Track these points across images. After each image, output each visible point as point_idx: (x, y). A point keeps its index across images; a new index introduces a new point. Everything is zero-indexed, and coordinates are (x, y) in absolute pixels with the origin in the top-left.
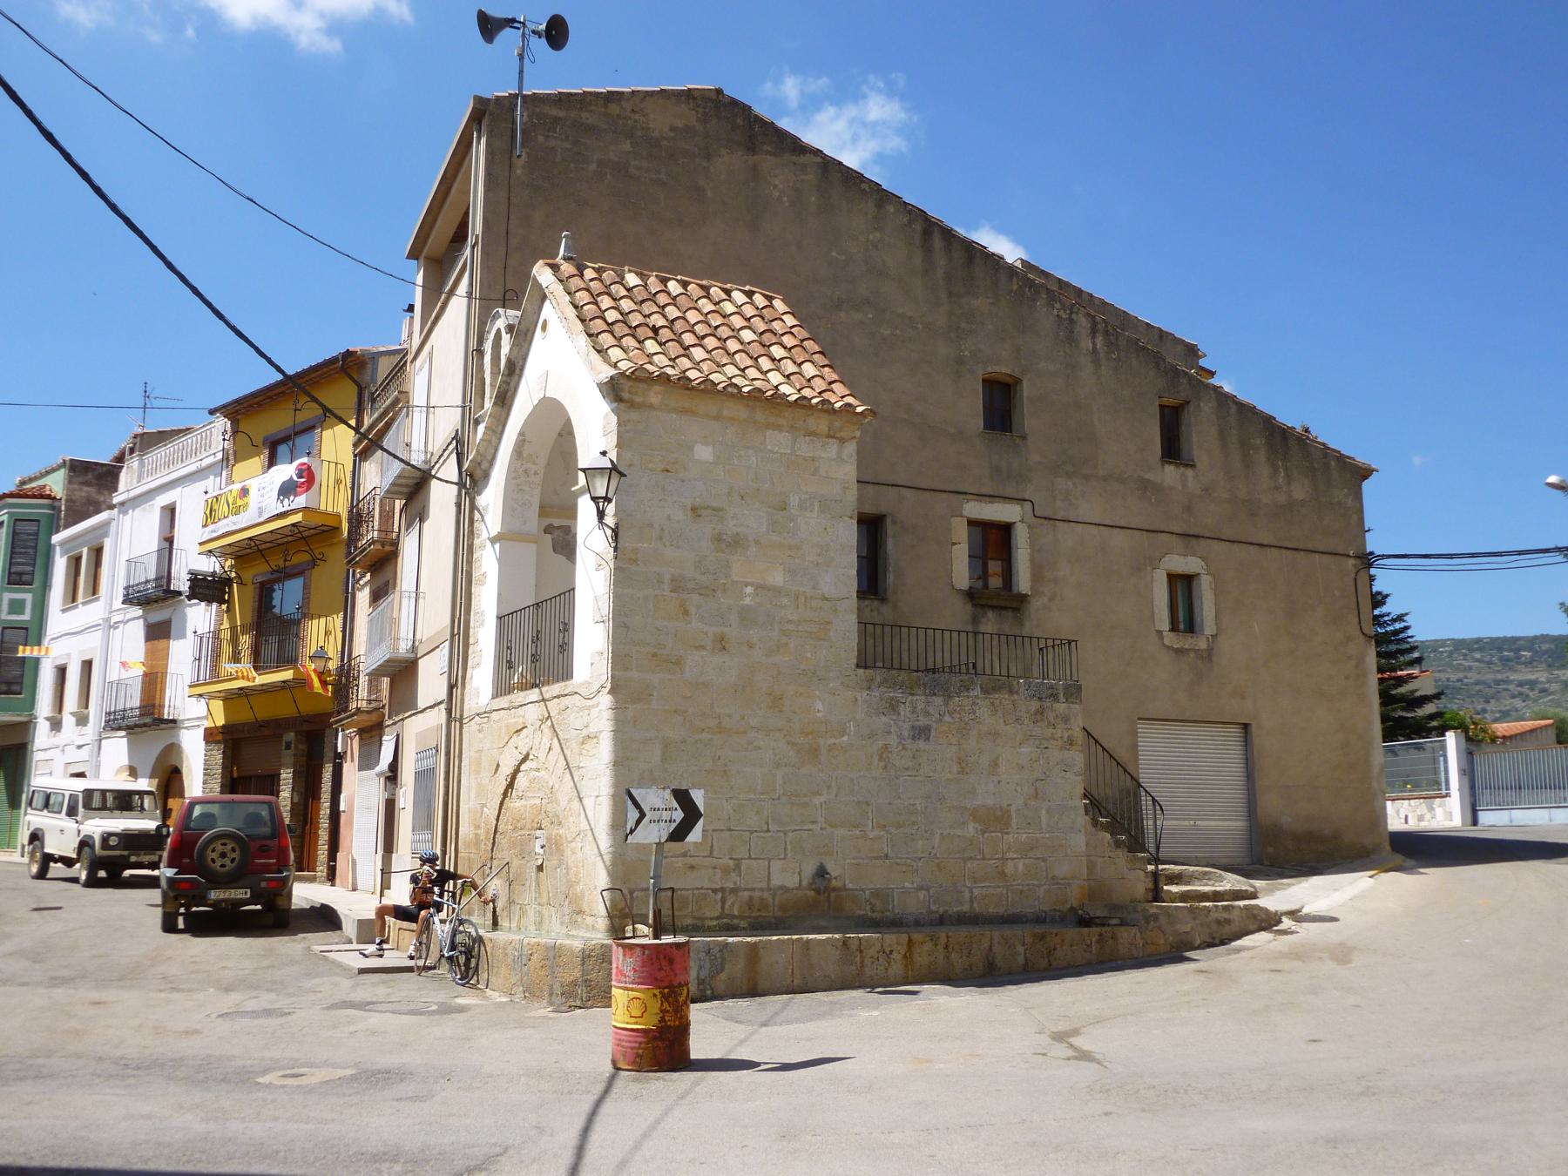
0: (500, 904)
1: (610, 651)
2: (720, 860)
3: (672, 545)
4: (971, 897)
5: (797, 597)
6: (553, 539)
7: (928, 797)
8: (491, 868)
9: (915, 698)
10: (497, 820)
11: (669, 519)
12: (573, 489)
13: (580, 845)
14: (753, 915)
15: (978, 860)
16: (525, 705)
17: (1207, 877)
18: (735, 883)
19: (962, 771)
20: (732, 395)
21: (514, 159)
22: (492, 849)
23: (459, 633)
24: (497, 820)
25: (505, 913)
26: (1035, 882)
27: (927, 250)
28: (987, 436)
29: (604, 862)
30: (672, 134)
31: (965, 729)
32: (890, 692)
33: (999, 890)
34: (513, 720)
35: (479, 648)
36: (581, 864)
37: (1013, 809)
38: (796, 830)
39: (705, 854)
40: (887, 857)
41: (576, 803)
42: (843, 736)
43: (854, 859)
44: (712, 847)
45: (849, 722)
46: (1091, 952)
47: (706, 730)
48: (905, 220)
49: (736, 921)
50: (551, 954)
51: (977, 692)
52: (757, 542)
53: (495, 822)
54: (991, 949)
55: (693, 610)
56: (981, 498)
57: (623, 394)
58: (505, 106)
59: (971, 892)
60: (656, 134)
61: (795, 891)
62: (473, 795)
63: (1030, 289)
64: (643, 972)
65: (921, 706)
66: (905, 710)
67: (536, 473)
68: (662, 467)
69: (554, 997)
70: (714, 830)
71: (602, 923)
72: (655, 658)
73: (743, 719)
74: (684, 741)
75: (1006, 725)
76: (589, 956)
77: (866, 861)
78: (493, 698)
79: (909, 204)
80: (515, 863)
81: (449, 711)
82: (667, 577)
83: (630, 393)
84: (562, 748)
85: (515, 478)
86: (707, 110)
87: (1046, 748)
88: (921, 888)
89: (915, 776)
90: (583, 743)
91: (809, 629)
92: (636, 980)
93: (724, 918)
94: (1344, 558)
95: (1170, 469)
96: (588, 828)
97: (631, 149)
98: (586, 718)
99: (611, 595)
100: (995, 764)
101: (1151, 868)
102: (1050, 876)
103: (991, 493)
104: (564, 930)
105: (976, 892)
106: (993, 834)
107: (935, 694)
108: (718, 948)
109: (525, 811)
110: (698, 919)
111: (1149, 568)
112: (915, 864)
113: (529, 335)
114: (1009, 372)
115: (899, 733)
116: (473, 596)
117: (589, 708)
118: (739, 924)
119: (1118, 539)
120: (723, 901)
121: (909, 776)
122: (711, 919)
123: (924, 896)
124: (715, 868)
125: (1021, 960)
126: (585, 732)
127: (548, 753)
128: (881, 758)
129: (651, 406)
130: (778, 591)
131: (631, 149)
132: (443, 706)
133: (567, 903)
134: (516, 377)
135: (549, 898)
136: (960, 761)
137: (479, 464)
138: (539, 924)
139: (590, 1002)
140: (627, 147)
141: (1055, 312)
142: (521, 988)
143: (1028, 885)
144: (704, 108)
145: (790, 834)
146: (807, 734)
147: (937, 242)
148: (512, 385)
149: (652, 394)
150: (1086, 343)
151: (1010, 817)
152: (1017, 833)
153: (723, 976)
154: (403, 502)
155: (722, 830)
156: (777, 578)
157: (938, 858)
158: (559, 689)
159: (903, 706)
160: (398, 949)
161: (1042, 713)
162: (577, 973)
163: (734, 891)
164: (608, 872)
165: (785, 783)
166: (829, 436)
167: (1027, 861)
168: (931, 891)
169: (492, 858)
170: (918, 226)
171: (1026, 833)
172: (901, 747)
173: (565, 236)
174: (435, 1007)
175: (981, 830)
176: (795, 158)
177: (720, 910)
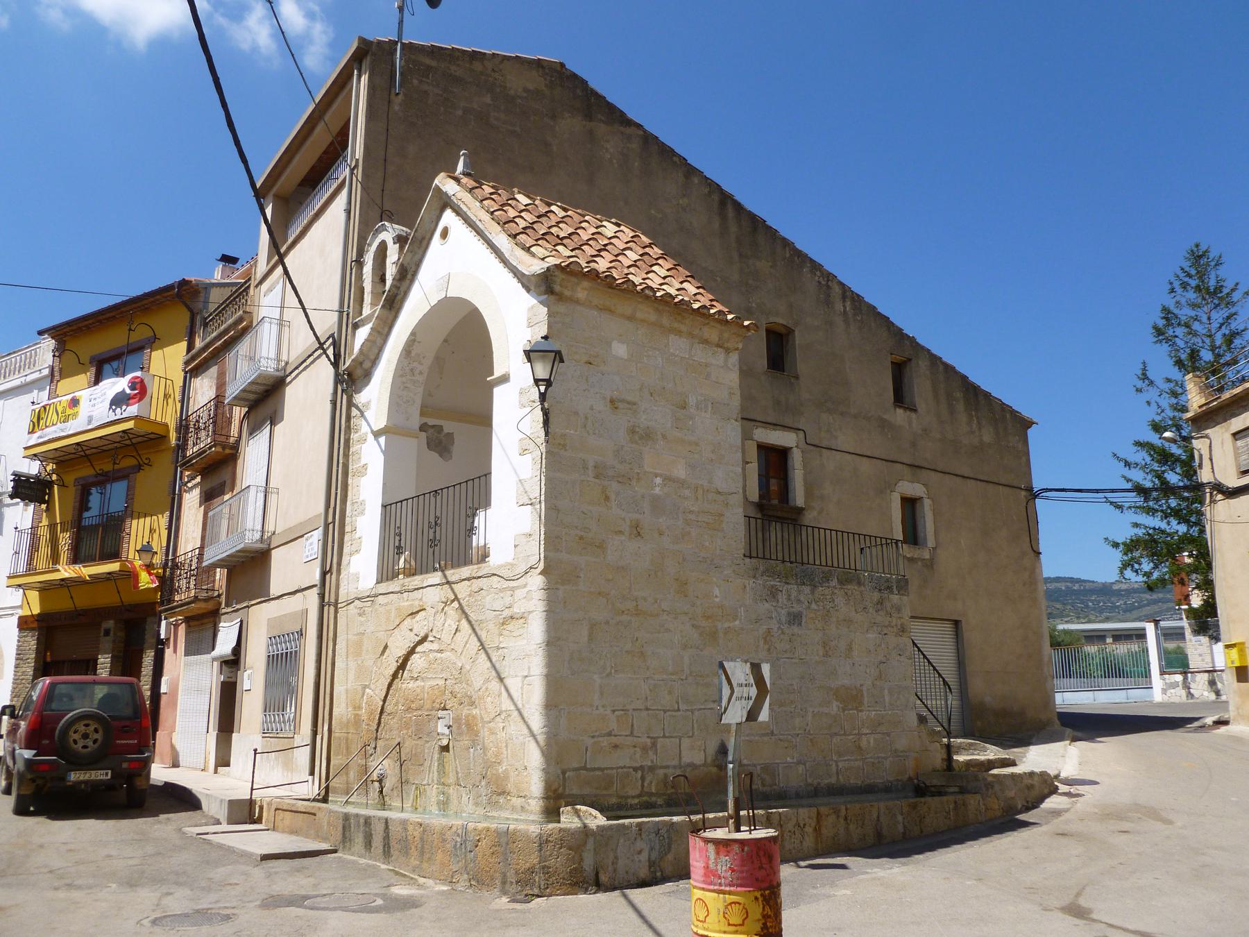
0: (388, 784)
1: (542, 533)
2: (640, 739)
3: (594, 434)
4: (837, 769)
5: (696, 488)
6: (427, 437)
7: (802, 678)
8: (375, 748)
9: (789, 587)
10: (384, 701)
11: (592, 409)
12: (488, 379)
13: (501, 725)
14: (669, 792)
15: (840, 735)
16: (422, 588)
17: (973, 748)
18: (652, 761)
19: (826, 655)
20: (647, 297)
21: (393, 96)
23: (334, 522)
24: (384, 701)
25: (395, 793)
26: (883, 755)
27: (723, 217)
28: (769, 374)
29: (537, 742)
30: (525, 95)
31: (827, 615)
32: (771, 581)
33: (857, 763)
34: (406, 604)
35: (357, 536)
36: (504, 744)
37: (864, 689)
38: (701, 709)
39: (627, 734)
40: (772, 733)
41: (495, 685)
42: (735, 620)
43: (747, 736)
44: (632, 725)
45: (740, 608)
46: (950, 818)
47: (626, 612)
48: (706, 191)
49: (654, 799)
50: (504, 840)
51: (834, 583)
52: (664, 437)
53: (381, 703)
54: (878, 820)
55: (613, 497)
56: (768, 425)
57: (555, 286)
58: (387, 49)
59: (837, 766)
60: (512, 92)
61: (702, 768)
62: (351, 676)
63: (798, 258)
64: (742, 872)
65: (794, 594)
66: (782, 598)
67: (421, 373)
68: (585, 358)
70: (634, 709)
71: (536, 805)
72: (582, 541)
73: (656, 602)
74: (607, 623)
75: (857, 613)
76: (547, 842)
77: (757, 738)
78: (377, 583)
79: (708, 178)
80: (408, 745)
81: (322, 596)
82: (591, 464)
83: (561, 286)
84: (474, 630)
85: (401, 376)
86: (553, 79)
87: (886, 634)
88: (799, 763)
89: (792, 658)
90: (503, 624)
91: (706, 520)
92: (735, 882)
93: (644, 796)
94: (1019, 490)
95: (900, 411)
96: (513, 708)
97: (491, 103)
98: (508, 600)
99: (543, 478)
100: (850, 648)
101: (945, 740)
102: (893, 748)
103: (774, 422)
104: (480, 811)
105: (841, 765)
106: (851, 712)
107: (804, 584)
108: (665, 829)
109: (423, 692)
110: (622, 797)
111: (888, 491)
112: (794, 740)
113: (425, 242)
114: (785, 323)
115: (778, 618)
116: (350, 488)
117: (513, 589)
118: (656, 801)
119: (866, 466)
120: (643, 779)
121: (788, 658)
122: (633, 797)
123: (802, 770)
124: (635, 747)
125: (901, 829)
126: (507, 613)
127: (455, 634)
128: (766, 642)
129: (577, 302)
130: (681, 483)
131: (491, 103)
132: (315, 591)
133: (483, 783)
134: (408, 282)
135: (458, 779)
136: (825, 645)
137: (361, 364)
138: (444, 805)
139: (548, 890)
140: (488, 99)
141: (817, 278)
142: (466, 876)
143: (878, 758)
144: (551, 77)
145: (696, 713)
146: (709, 617)
147: (731, 212)
148: (402, 289)
149: (579, 289)
150: (839, 306)
151: (862, 695)
152: (869, 711)
153: (670, 857)
154: (245, 410)
155: (640, 710)
156: (680, 472)
157: (810, 735)
158: (469, 572)
159: (780, 593)
160: (274, 830)
161: (882, 603)
162: (534, 859)
163: (652, 769)
164: (542, 752)
165: (691, 664)
166: (718, 346)
167: (877, 736)
168: (807, 765)
169: (376, 738)
170: (716, 197)
171: (874, 711)
172: (780, 632)
173: (463, 154)
174: (379, 902)
175: (842, 708)
176: (622, 129)
177: (640, 788)
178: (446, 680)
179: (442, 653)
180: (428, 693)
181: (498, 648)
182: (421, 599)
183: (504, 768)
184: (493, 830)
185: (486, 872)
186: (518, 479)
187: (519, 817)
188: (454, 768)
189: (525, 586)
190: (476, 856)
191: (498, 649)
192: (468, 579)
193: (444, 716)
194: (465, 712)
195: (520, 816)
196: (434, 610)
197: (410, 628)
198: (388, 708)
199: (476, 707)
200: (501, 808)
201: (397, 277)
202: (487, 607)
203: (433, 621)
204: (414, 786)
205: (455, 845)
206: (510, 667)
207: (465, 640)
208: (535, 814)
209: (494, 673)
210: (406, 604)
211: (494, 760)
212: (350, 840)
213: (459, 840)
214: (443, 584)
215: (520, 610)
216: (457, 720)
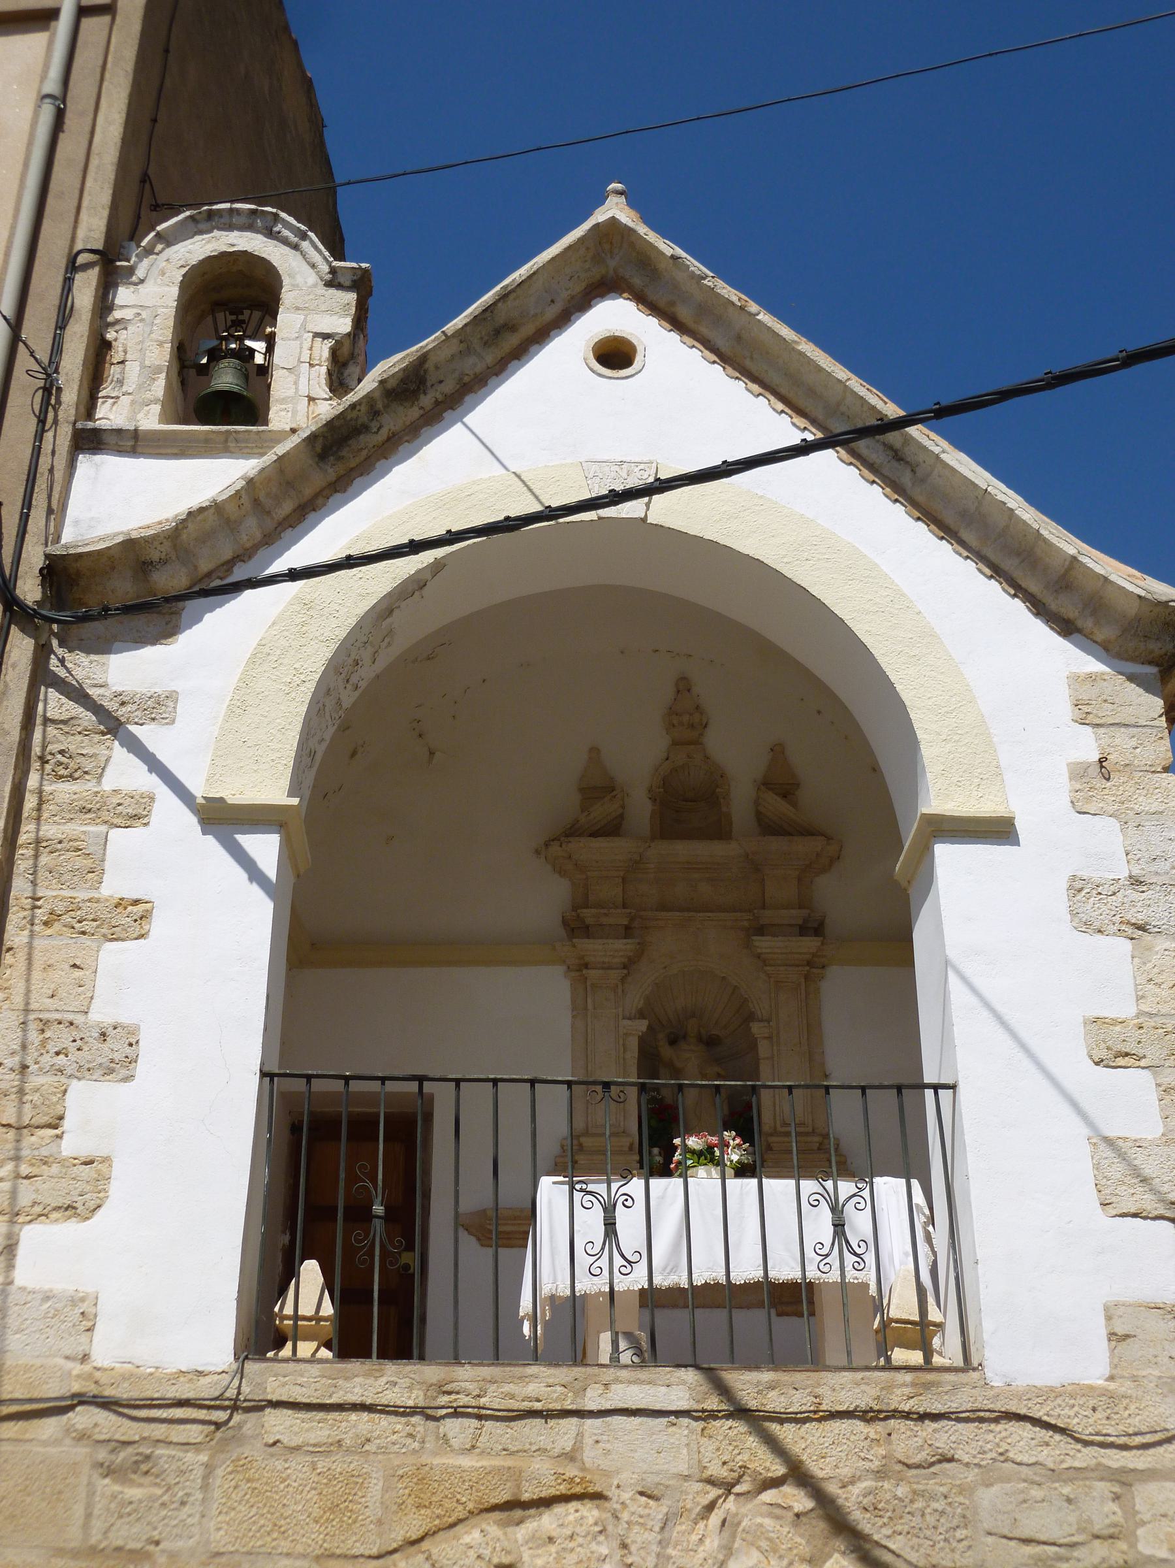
35: (72, 1145)
113: (513, 340)
117: (1124, 1479)
134: (414, 413)
158: (874, 1392)
182: (571, 1456)
192: (867, 1416)
196: (658, 1511)
201: (391, 384)
202: (986, 1526)
203: (655, 1548)
210: (466, 1462)
214: (712, 1415)
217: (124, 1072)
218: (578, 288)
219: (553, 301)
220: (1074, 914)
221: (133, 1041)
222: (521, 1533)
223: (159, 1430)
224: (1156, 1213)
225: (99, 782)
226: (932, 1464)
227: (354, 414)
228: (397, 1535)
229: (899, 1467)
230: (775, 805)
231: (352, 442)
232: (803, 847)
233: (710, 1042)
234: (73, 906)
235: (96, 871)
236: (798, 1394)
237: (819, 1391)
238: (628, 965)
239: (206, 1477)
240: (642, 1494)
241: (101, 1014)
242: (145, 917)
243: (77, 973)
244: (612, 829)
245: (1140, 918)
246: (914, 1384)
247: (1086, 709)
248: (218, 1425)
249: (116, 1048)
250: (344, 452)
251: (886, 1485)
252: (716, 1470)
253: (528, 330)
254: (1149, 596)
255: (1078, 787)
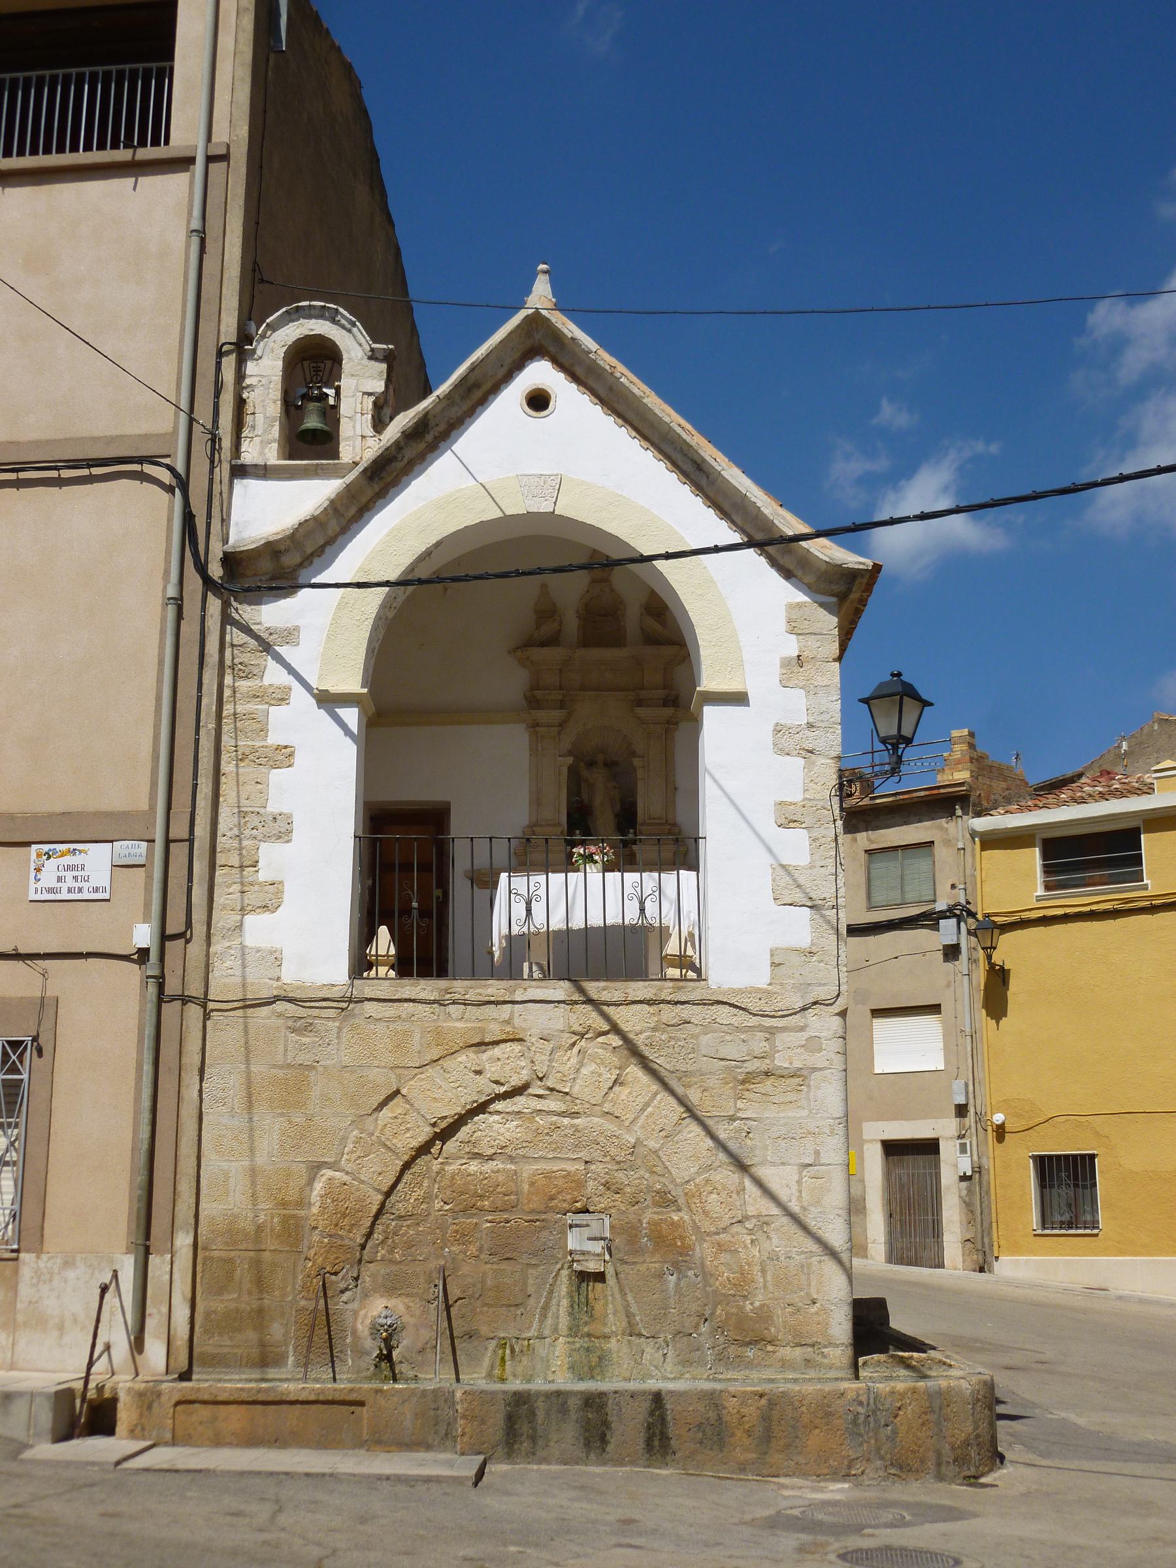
22: (363, 1247)
35: (263, 875)
36: (757, 1268)
41: (727, 1176)
69: (943, 1468)
90: (743, 1082)
96: (775, 1211)
98: (759, 1044)
113: (478, 394)
117: (772, 1031)
134: (422, 446)
142: (879, 1463)
158: (654, 991)
178: (586, 1162)
179: (573, 1118)
180: (532, 1184)
181: (732, 1119)
182: (508, 1022)
183: (757, 1304)
184: (922, 1390)
185: (913, 1452)
186: (775, 865)
187: (798, 1376)
188: (620, 1308)
189: (802, 1029)
190: (895, 1432)
191: (734, 1120)
192: (650, 1002)
193: (585, 1223)
194: (649, 1216)
195: (802, 1373)
196: (548, 1046)
197: (478, 1068)
198: (401, 1203)
199: (680, 1210)
200: (750, 1365)
204: (493, 1343)
205: (855, 1422)
206: (766, 1148)
207: (641, 1100)
208: (841, 1368)
209: (722, 1156)
210: (459, 1025)
211: (731, 1292)
212: (533, 1439)
213: (861, 1410)
214: (576, 1003)
215: (791, 1064)
216: (629, 1231)
217: (286, 838)
218: (517, 355)
219: (502, 366)
220: (775, 745)
221: (290, 822)
222: (485, 1056)
223: (316, 1012)
224: (801, 903)
225: (262, 680)
226: (680, 1025)
227: (388, 452)
228: (428, 1058)
229: (663, 1026)
230: (653, 624)
231: (388, 468)
232: (666, 651)
233: (610, 765)
234: (254, 750)
235: (263, 730)
236: (617, 992)
237: (627, 991)
238: (562, 725)
239: (339, 1033)
240: (541, 1039)
241: (273, 808)
242: (291, 755)
243: (259, 786)
244: (552, 641)
245: (810, 747)
246: (673, 988)
247: (793, 624)
248: (343, 1009)
249: (281, 826)
250: (384, 475)
251: (657, 1034)
252: (576, 1028)
253: (487, 386)
254: (831, 561)
255: (784, 672)
